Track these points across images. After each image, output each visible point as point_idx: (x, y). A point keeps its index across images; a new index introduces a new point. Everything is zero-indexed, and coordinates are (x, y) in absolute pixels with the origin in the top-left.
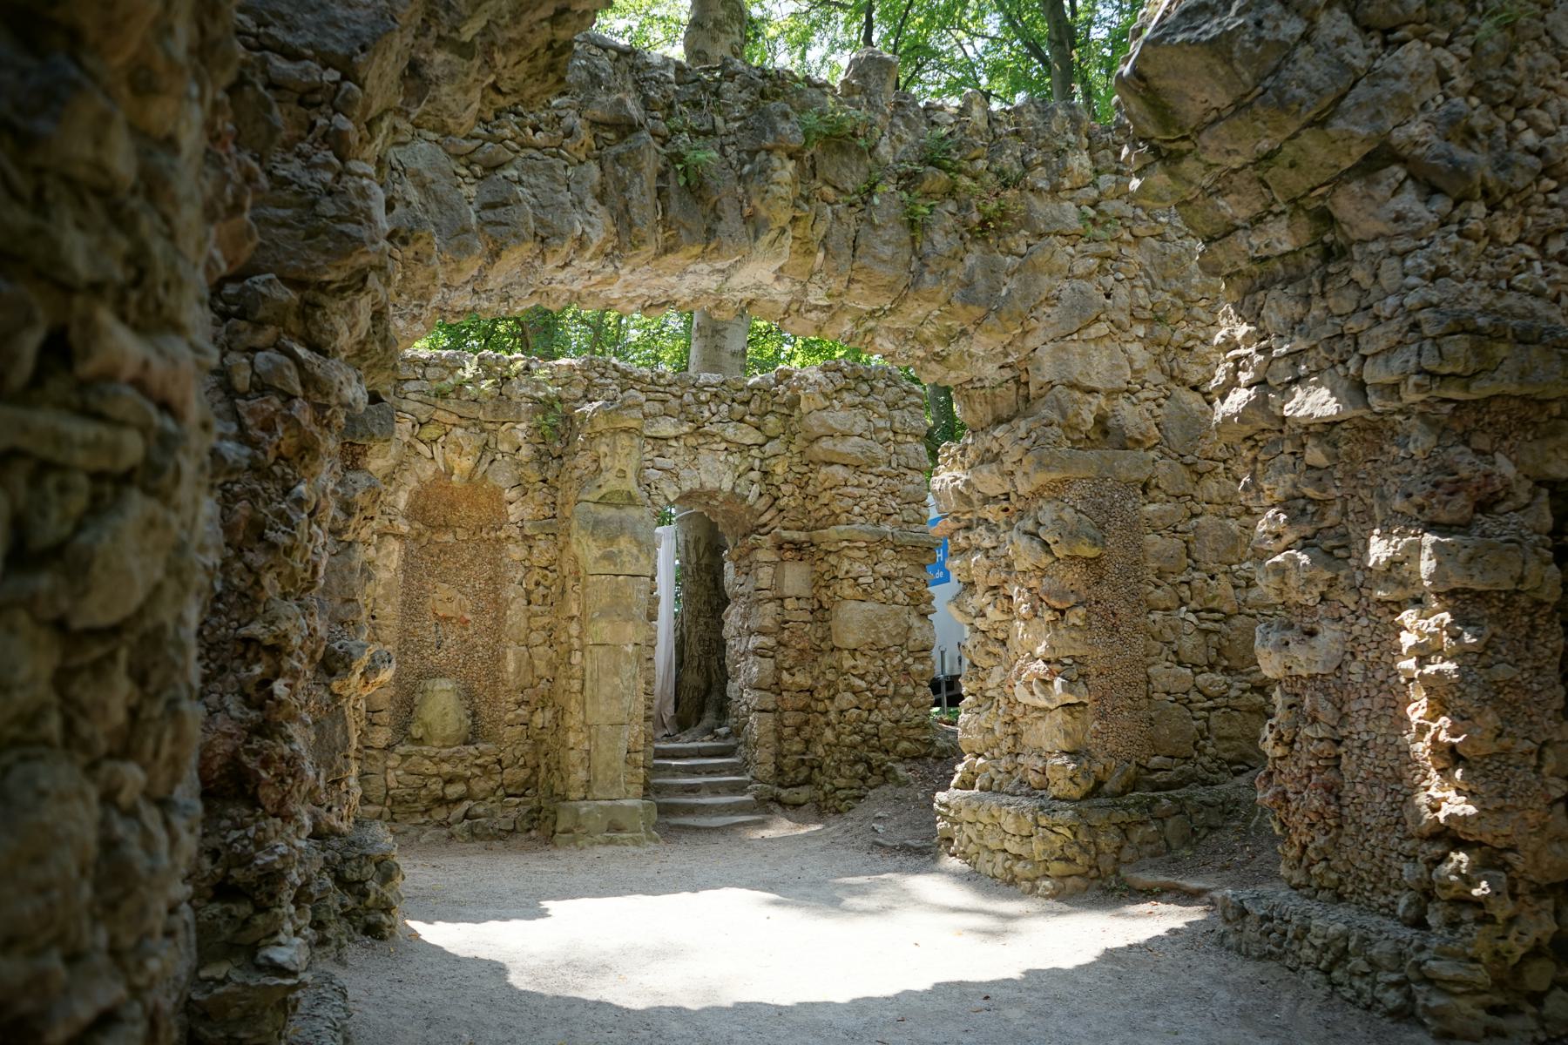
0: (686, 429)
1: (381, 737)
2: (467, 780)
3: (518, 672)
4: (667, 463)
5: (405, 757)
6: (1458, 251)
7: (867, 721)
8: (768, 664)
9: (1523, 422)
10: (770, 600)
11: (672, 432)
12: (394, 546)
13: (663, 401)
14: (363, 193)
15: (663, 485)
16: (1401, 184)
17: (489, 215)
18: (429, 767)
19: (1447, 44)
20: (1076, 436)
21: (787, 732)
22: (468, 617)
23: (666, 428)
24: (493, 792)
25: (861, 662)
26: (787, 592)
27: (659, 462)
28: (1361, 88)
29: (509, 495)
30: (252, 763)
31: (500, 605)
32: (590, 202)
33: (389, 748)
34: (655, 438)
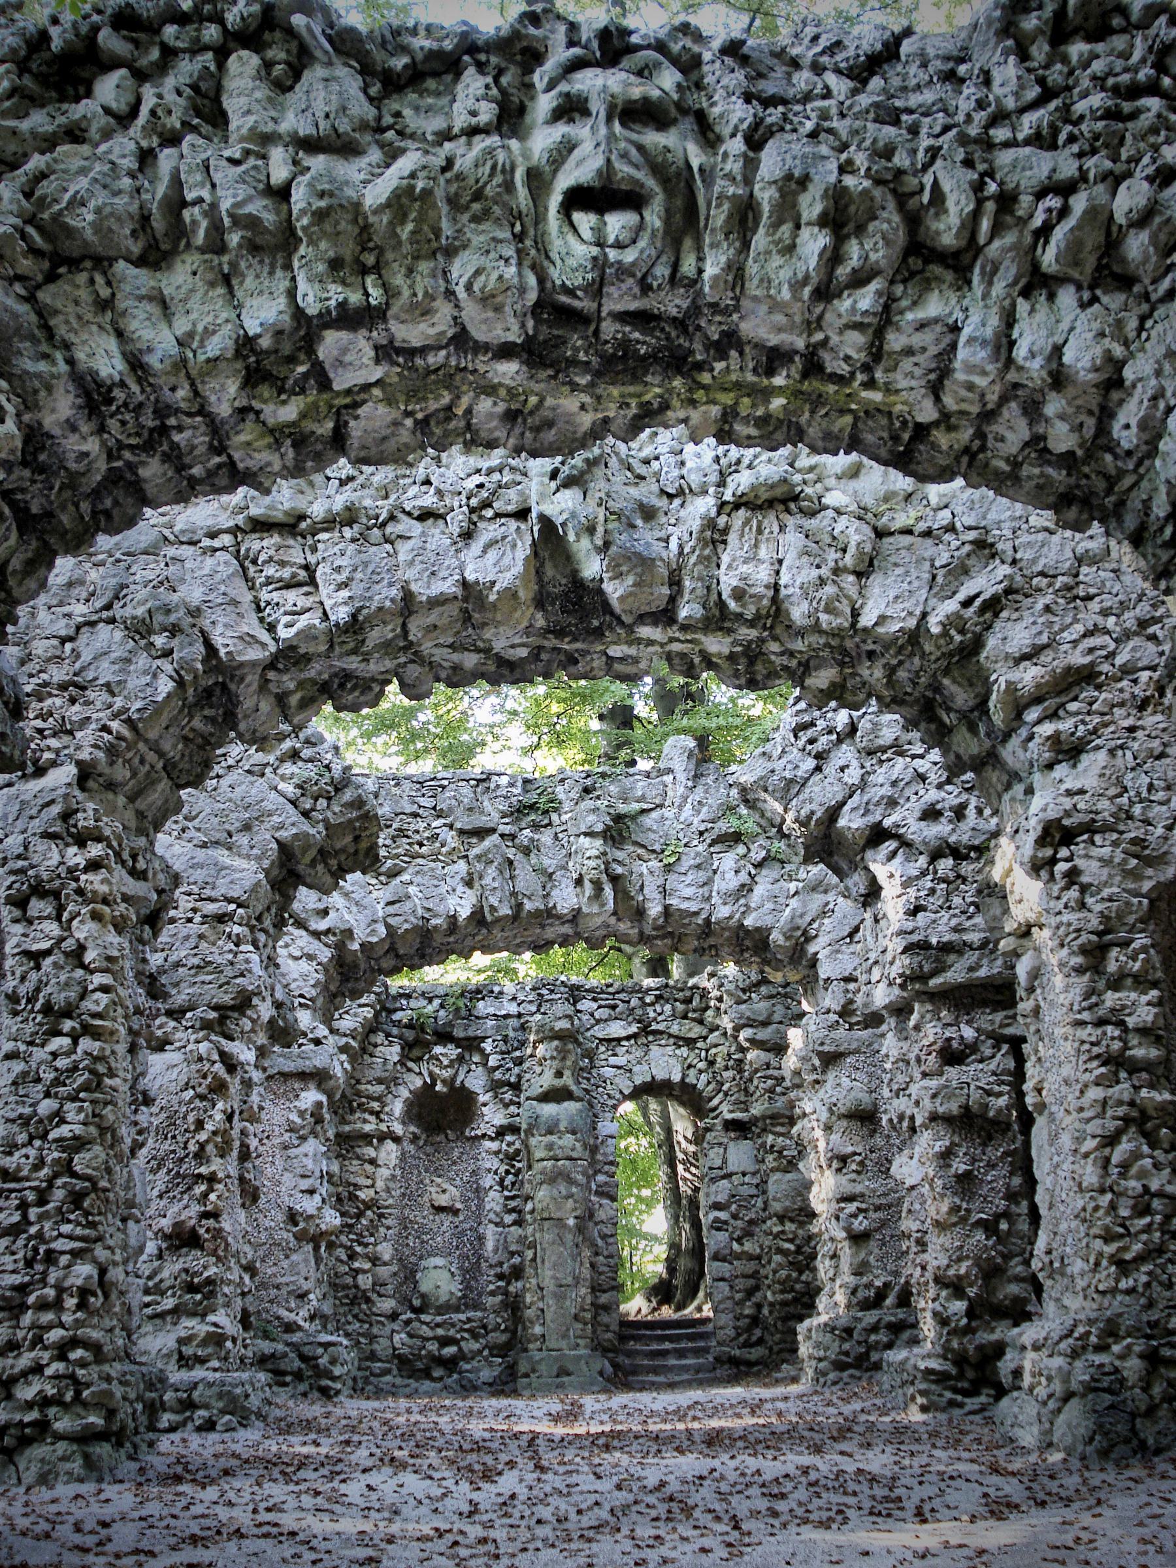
0: (634, 1029)
1: (387, 1305)
2: (455, 1342)
3: (496, 1251)
4: (620, 1061)
5: (408, 1322)
6: (932, 891)
7: (797, 1281)
8: (722, 1236)
9: (984, 1003)
10: (723, 1177)
11: (624, 1034)
12: (390, 1145)
13: (614, 1007)
14: (247, 961)
15: (617, 1080)
16: (894, 854)
17: (391, 909)
18: (425, 1331)
19: (922, 757)
20: (854, 1020)
21: (738, 1296)
22: (458, 1206)
23: (617, 1029)
24: (480, 1352)
25: (790, 1227)
26: (731, 1168)
27: (613, 1060)
28: (856, 797)
29: (482, 1098)
30: (202, 1231)
31: (479, 1192)
32: (460, 888)
33: (394, 1316)
34: (609, 1041)
